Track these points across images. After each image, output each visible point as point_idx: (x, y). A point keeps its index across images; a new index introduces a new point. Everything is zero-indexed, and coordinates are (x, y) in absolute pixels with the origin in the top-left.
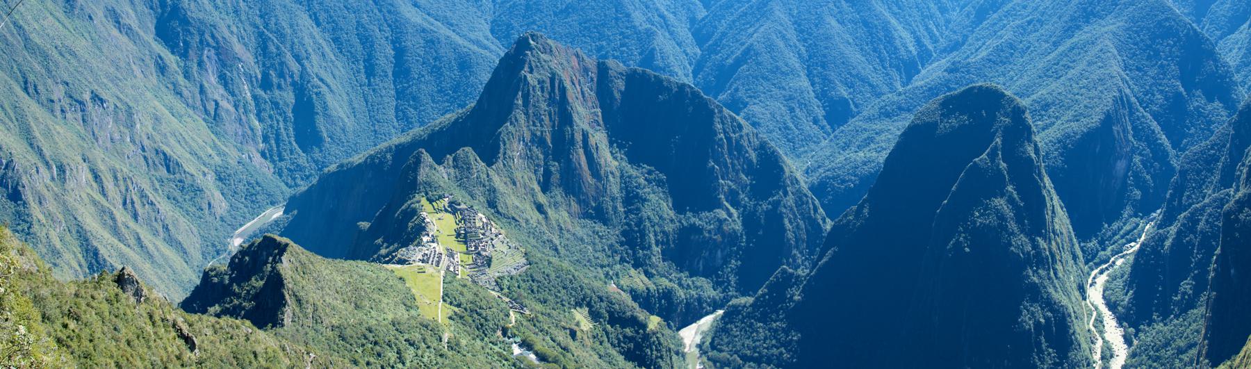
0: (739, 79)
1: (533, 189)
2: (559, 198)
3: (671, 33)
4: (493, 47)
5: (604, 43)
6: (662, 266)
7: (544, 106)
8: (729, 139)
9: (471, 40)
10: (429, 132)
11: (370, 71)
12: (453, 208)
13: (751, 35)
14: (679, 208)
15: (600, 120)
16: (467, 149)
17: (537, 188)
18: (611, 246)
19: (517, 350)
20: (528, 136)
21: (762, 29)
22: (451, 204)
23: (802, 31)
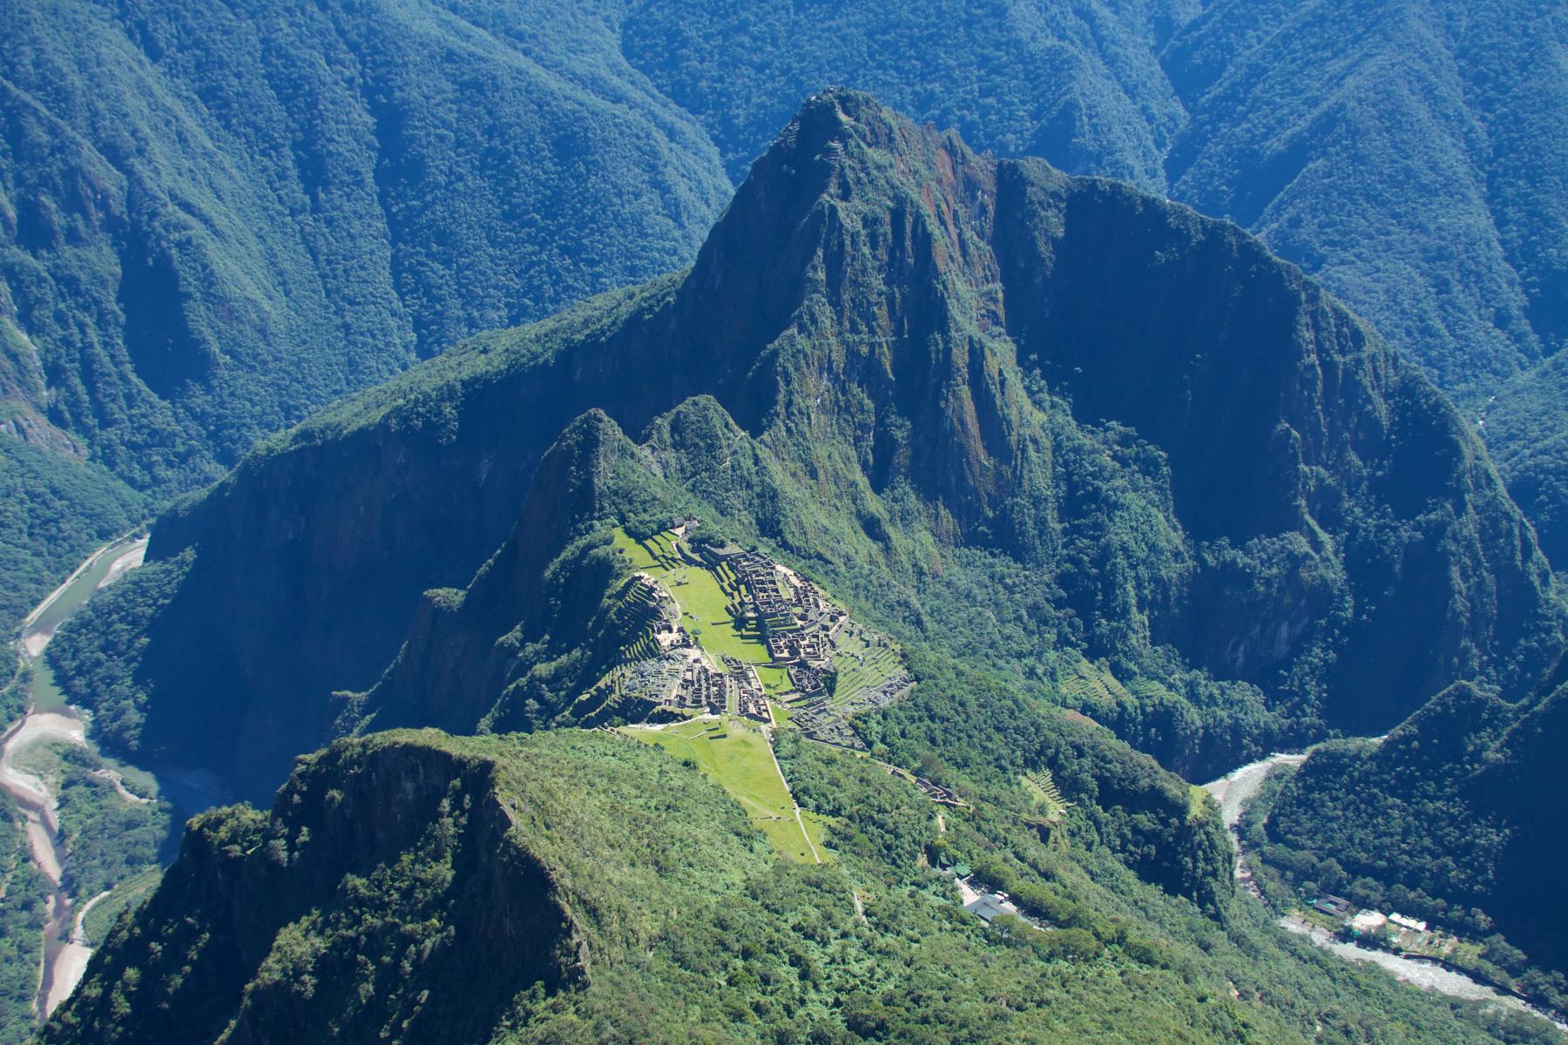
0: (1300, 194)
1: (853, 484)
2: (913, 502)
3: (1110, 61)
4: (637, 95)
5: (937, 88)
6: (1152, 656)
7: (877, 282)
8: (1329, 367)
9: (575, 78)
10: (557, 344)
11: (314, 172)
12: (705, 552)
13: (1338, 80)
14: (1199, 521)
15: (1001, 313)
16: (702, 399)
17: (862, 481)
18: (1034, 609)
19: (970, 896)
20: (839, 357)
21: (1370, 67)
22: (698, 543)
23: (1480, 80)
